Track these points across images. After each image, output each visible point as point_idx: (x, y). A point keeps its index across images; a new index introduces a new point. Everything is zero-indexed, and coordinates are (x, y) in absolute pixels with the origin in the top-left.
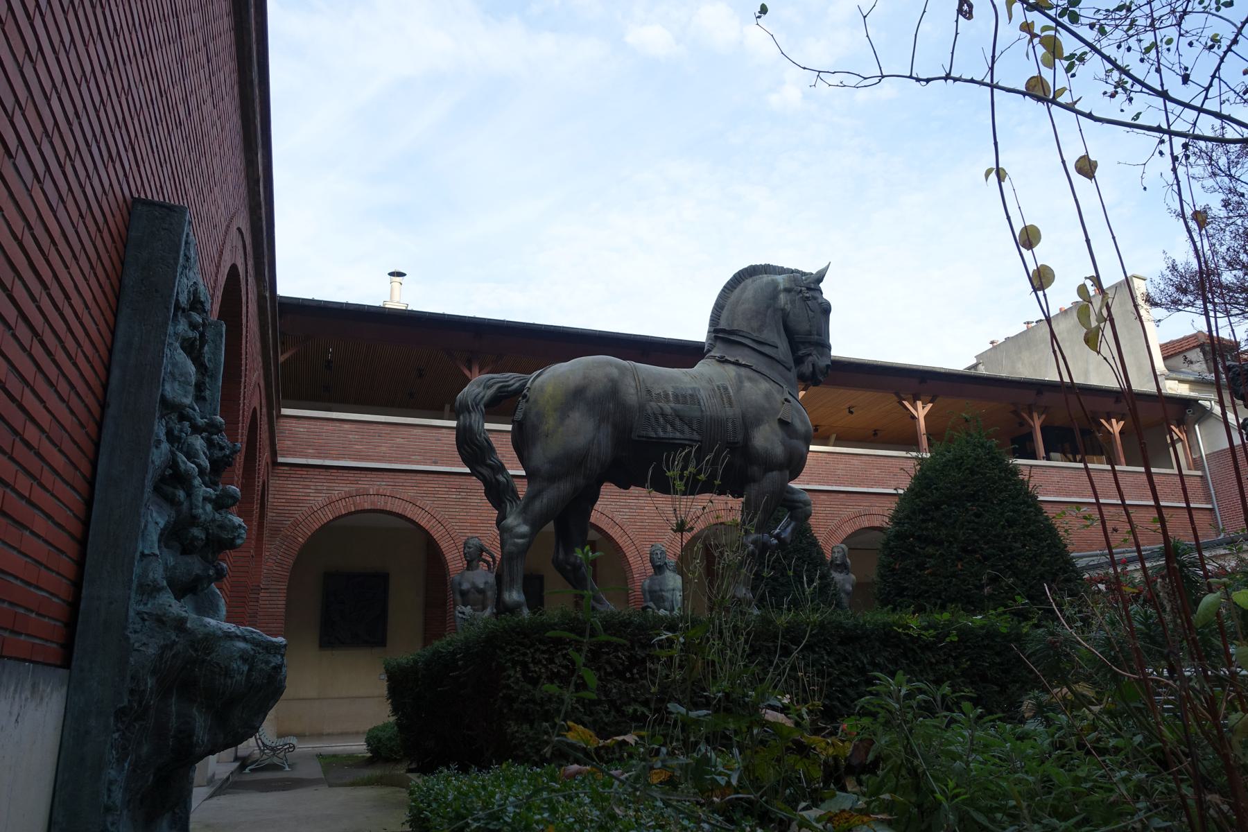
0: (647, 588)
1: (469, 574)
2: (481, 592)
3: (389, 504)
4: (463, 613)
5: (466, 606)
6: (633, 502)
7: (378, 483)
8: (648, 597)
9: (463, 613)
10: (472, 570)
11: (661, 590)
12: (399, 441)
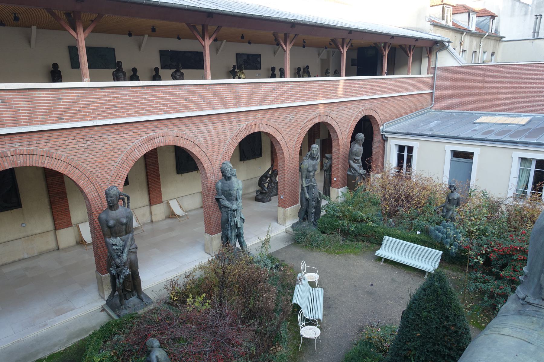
0: (220, 188)
1: (113, 214)
3: (28, 161)
4: (116, 245)
5: (116, 237)
6: (205, 128)
7: (14, 145)
8: (220, 192)
9: (116, 245)
10: (115, 210)
11: (230, 190)
12: (23, 104)
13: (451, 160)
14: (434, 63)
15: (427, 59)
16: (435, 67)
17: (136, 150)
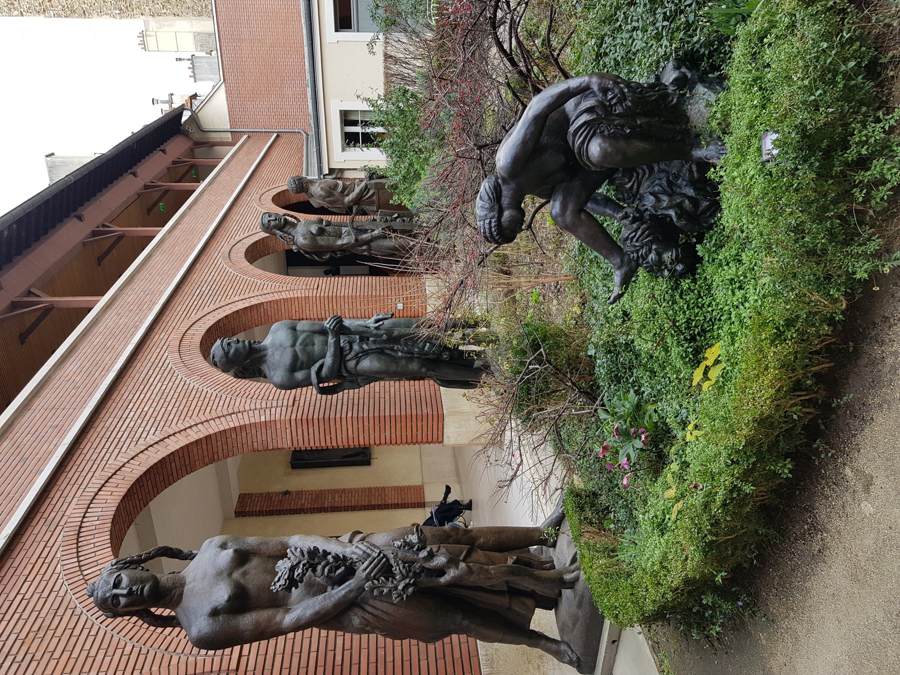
2: (242, 557)
8: (300, 375)
10: (183, 585)
13: (358, 31)
14: (223, 135)
15: (217, 148)
16: (231, 132)
17: (85, 573)
